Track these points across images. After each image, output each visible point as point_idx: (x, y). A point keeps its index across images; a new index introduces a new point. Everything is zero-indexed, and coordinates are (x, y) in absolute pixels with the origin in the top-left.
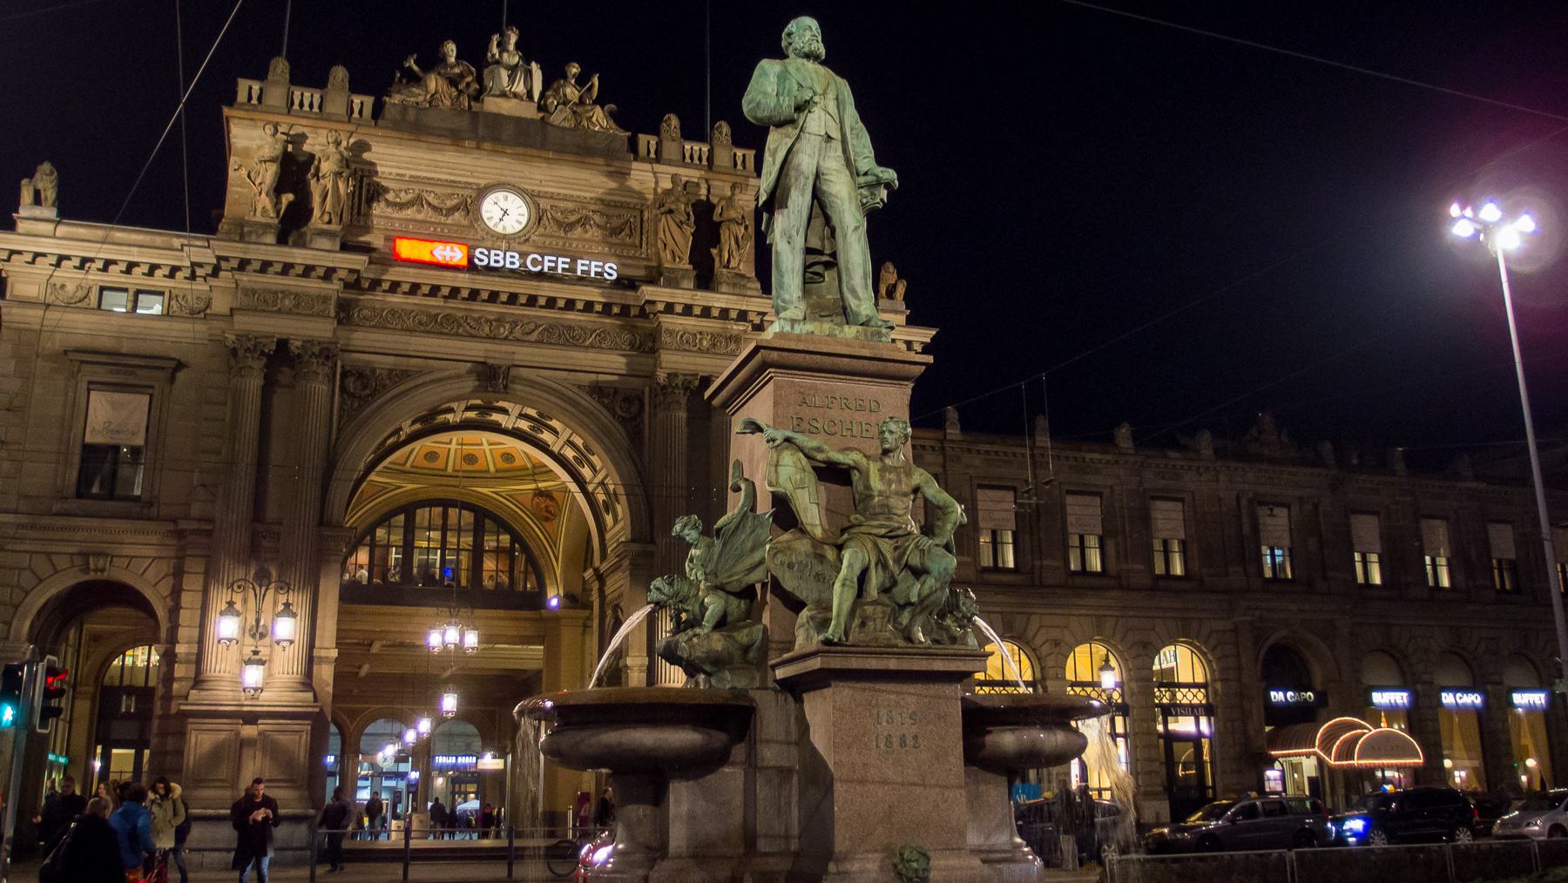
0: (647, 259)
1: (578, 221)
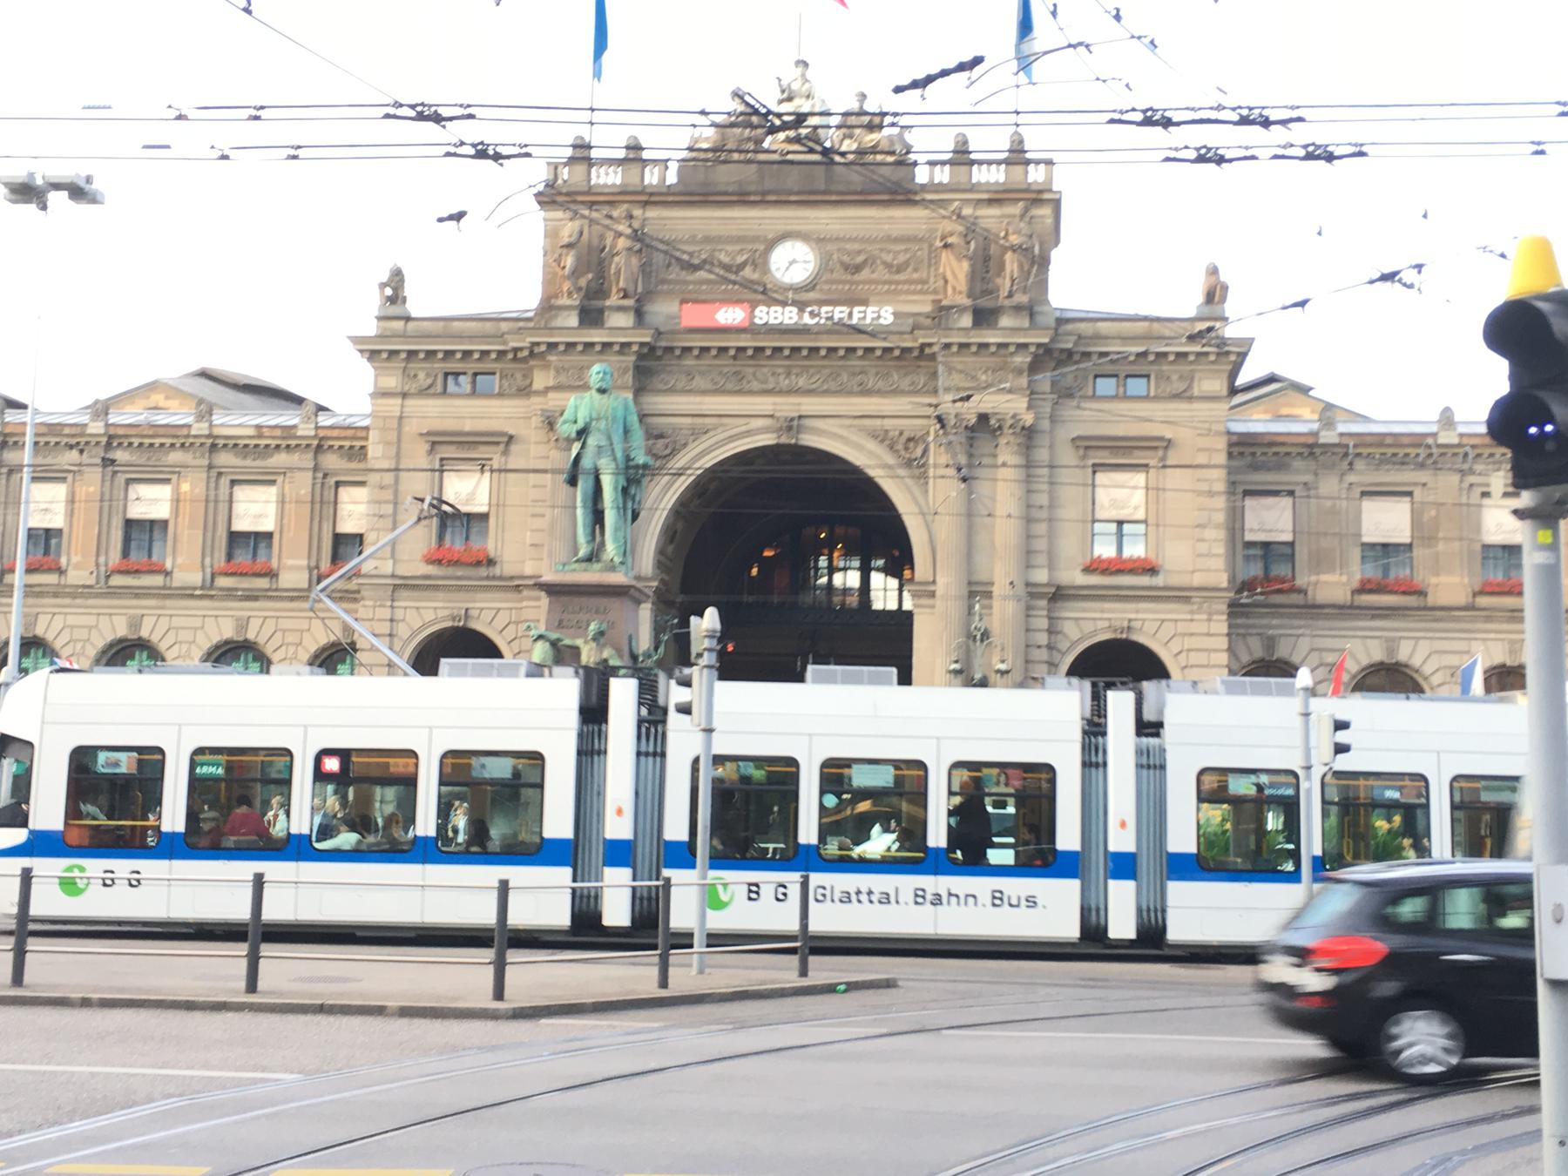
0: (935, 292)
1: (865, 261)
